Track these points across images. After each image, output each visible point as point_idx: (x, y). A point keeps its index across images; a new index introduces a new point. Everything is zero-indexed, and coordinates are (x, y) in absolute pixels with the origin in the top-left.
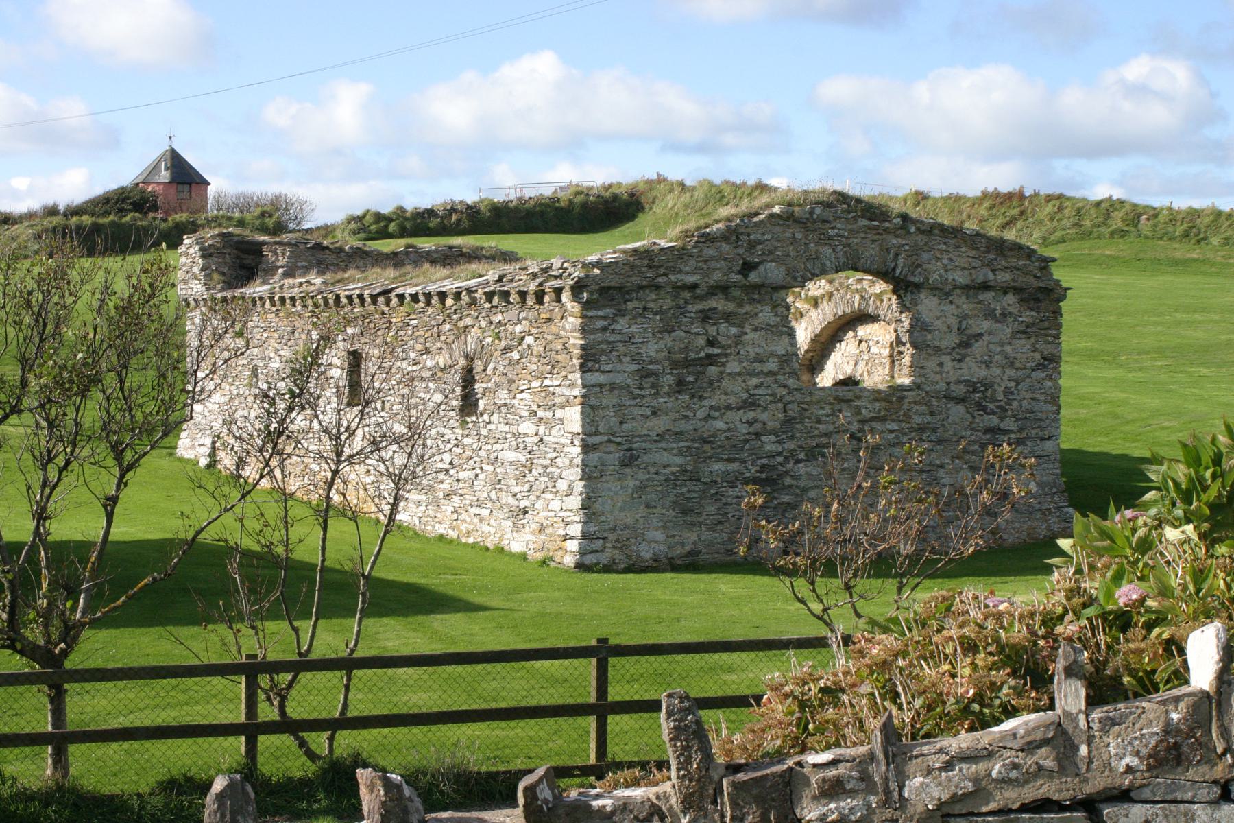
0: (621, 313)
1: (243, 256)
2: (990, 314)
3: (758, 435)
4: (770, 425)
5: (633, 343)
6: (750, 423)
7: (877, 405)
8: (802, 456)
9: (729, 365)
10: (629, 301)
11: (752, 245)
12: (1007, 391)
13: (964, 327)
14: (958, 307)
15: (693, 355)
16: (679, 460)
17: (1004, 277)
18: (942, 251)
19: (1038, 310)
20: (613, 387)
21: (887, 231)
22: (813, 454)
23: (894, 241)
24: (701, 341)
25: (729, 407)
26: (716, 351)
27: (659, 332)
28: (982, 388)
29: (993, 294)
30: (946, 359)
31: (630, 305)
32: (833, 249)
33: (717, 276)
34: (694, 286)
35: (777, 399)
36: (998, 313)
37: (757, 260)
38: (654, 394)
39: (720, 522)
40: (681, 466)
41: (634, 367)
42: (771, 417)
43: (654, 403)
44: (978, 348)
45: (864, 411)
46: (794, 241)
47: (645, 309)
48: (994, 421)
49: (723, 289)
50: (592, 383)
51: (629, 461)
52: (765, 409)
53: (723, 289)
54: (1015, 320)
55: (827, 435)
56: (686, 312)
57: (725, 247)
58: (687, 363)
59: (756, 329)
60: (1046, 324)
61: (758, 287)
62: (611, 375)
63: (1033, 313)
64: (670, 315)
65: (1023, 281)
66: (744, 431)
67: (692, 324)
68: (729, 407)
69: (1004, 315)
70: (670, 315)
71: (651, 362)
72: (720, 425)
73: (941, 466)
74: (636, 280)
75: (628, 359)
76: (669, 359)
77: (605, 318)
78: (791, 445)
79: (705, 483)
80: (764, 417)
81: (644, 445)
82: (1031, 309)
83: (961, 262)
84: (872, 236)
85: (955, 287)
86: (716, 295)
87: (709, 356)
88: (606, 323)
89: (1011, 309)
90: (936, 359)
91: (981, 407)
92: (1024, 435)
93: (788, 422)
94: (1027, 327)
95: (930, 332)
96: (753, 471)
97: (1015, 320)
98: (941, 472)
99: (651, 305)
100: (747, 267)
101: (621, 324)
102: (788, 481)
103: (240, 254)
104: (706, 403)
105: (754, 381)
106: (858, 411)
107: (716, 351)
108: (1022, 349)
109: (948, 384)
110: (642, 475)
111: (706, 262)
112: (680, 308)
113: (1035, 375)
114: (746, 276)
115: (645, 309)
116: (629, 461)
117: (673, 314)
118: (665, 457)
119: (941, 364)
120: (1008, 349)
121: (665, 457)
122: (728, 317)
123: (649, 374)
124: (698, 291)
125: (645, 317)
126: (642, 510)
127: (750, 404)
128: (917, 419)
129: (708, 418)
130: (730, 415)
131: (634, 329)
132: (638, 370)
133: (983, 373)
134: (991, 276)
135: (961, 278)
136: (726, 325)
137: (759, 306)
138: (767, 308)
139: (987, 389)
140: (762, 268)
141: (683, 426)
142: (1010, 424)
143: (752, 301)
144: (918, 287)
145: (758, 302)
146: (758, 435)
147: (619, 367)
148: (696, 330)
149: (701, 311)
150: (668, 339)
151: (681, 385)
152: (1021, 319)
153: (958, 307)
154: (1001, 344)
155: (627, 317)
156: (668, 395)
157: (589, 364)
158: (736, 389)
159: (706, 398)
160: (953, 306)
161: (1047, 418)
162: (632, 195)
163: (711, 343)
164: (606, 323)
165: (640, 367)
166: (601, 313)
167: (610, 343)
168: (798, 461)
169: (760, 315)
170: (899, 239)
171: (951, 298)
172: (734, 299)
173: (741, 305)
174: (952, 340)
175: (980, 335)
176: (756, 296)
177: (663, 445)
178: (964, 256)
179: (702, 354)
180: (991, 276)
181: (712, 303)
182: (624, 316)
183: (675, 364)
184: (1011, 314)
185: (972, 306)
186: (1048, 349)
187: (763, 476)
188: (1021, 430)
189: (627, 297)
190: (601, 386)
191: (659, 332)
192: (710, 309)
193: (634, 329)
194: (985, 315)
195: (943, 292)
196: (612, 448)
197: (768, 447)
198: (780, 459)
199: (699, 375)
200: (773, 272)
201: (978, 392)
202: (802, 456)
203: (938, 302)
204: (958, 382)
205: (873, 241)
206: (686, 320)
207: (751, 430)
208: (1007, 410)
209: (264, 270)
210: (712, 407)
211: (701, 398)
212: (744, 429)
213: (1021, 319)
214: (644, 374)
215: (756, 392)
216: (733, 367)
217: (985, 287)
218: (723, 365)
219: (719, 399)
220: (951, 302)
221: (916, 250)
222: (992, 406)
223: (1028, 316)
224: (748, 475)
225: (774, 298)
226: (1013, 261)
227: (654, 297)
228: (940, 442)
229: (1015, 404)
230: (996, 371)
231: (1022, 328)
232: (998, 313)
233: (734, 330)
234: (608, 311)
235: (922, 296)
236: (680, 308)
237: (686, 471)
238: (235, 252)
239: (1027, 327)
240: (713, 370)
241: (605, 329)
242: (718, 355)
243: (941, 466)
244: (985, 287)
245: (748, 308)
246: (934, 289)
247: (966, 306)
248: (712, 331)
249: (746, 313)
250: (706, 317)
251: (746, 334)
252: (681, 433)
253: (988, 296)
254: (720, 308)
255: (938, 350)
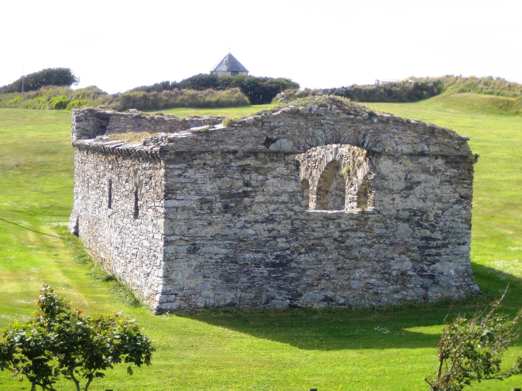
0: (191, 167)
1: (101, 121)
2: (426, 171)
3: (275, 238)
4: (282, 232)
5: (197, 184)
6: (270, 231)
7: (351, 222)
8: (303, 250)
9: (257, 197)
10: (195, 159)
11: (272, 129)
12: (436, 216)
13: (409, 177)
14: (405, 166)
15: (234, 191)
16: (224, 251)
17: (434, 149)
18: (394, 134)
19: (458, 168)
20: (184, 208)
21: (359, 121)
22: (310, 249)
23: (363, 127)
24: (240, 183)
25: (256, 222)
26: (249, 189)
27: (213, 178)
28: (420, 214)
29: (428, 158)
30: (397, 197)
31: (196, 162)
32: (324, 131)
33: (249, 146)
34: (235, 152)
35: (286, 218)
36: (431, 170)
37: (275, 137)
38: (210, 213)
39: (249, 287)
40: (226, 254)
41: (197, 197)
42: (284, 228)
43: (209, 218)
44: (418, 190)
45: (343, 226)
46: (298, 126)
47: (205, 164)
48: (428, 233)
49: (254, 153)
50: (171, 206)
51: (194, 250)
52: (280, 223)
53: (254, 153)
54: (443, 174)
55: (320, 239)
56: (231, 166)
57: (255, 130)
58: (231, 196)
59: (275, 177)
60: (463, 177)
61: (277, 153)
62: (183, 201)
63: (455, 170)
64: (220, 168)
65: (447, 151)
66: (266, 235)
67: (234, 173)
68: (256, 222)
69: (436, 171)
70: (220, 168)
71: (208, 195)
72: (251, 231)
73: (393, 259)
74: (198, 148)
75: (193, 193)
76: (220, 193)
77: (180, 169)
78: (296, 245)
79: (240, 265)
80: (279, 227)
81: (202, 242)
82: (453, 168)
83: (408, 139)
84: (349, 124)
85: (403, 154)
86: (250, 157)
87: (245, 192)
88: (181, 172)
89: (440, 168)
90: (391, 196)
91: (419, 225)
92: (447, 241)
93: (294, 231)
94: (451, 178)
95: (386, 180)
96: (271, 258)
97: (443, 174)
98: (392, 262)
99: (208, 162)
100: (269, 141)
101: (190, 172)
102: (293, 265)
103: (99, 120)
104: (243, 219)
105: (273, 207)
106: (339, 225)
107: (249, 189)
108: (447, 191)
109: (398, 211)
110: (201, 259)
111: (242, 138)
112: (227, 164)
113: (455, 207)
114: (268, 147)
115: (205, 164)
116: (194, 250)
117: (223, 168)
118: (216, 249)
119: (393, 199)
120: (438, 191)
121: (216, 249)
122: (257, 170)
123: (207, 202)
124: (238, 155)
125: (204, 169)
126: (200, 280)
127: (270, 220)
128: (377, 231)
129: (242, 228)
130: (258, 226)
131: (198, 176)
132: (200, 199)
133: (421, 205)
134: (426, 148)
135: (406, 149)
136: (256, 174)
137: (277, 164)
138: (282, 165)
139: (423, 215)
140: (278, 142)
141: (227, 231)
142: (437, 235)
143: (272, 161)
144: (380, 154)
145: (276, 161)
146: (275, 238)
147: (188, 197)
148: (237, 177)
149: (240, 166)
150: (219, 182)
151: (226, 208)
152: (446, 174)
153: (405, 166)
154: (433, 188)
155: (194, 169)
156: (218, 213)
157: (170, 195)
158: (262, 211)
159: (242, 216)
160: (402, 166)
161: (463, 232)
162: (439, 81)
163: (247, 184)
164: (181, 172)
165: (201, 197)
166: (177, 166)
167: (182, 183)
168: (300, 254)
169: (278, 169)
170: (367, 126)
171: (400, 161)
172: (261, 160)
173: (265, 163)
174: (401, 185)
175: (419, 183)
176: (275, 158)
177: (215, 242)
178: (410, 135)
179: (240, 191)
180: (426, 148)
181: (248, 161)
182: (192, 168)
183: (223, 196)
184: (440, 170)
185: (414, 165)
186: (464, 191)
187: (278, 261)
188: (445, 239)
189: (194, 157)
190: (177, 208)
191: (213, 178)
192: (246, 165)
193: (198, 176)
194: (423, 171)
195: (394, 157)
196: (183, 243)
197: (281, 245)
198: (288, 252)
199: (237, 203)
200: (285, 144)
201: (417, 216)
202: (303, 250)
203: (392, 163)
204: (404, 210)
205: (350, 127)
206: (231, 171)
207: (270, 235)
208: (436, 227)
209: (109, 129)
210: (246, 221)
211: (239, 216)
212: (266, 234)
213: (446, 174)
214: (203, 201)
215: (274, 213)
216: (259, 198)
217: (423, 154)
218: (253, 197)
219: (250, 217)
220: (401, 163)
221: (377, 132)
222: (426, 224)
223: (451, 172)
224: (268, 260)
225: (286, 160)
226: (441, 139)
227: (210, 157)
228: (391, 244)
229: (441, 224)
230: (429, 203)
231: (448, 179)
232: (431, 170)
233: (260, 177)
234: (183, 165)
235: (382, 159)
236: (227, 164)
237: (229, 257)
238: (97, 119)
239: (451, 178)
240: (247, 200)
241: (180, 175)
242: (250, 192)
243: (393, 259)
244: (423, 154)
245: (270, 165)
246: (390, 156)
247: (410, 165)
248: (247, 177)
249: (268, 168)
250: (243, 169)
251: (268, 179)
252: (226, 235)
253: (424, 160)
254: (252, 164)
255: (391, 191)
